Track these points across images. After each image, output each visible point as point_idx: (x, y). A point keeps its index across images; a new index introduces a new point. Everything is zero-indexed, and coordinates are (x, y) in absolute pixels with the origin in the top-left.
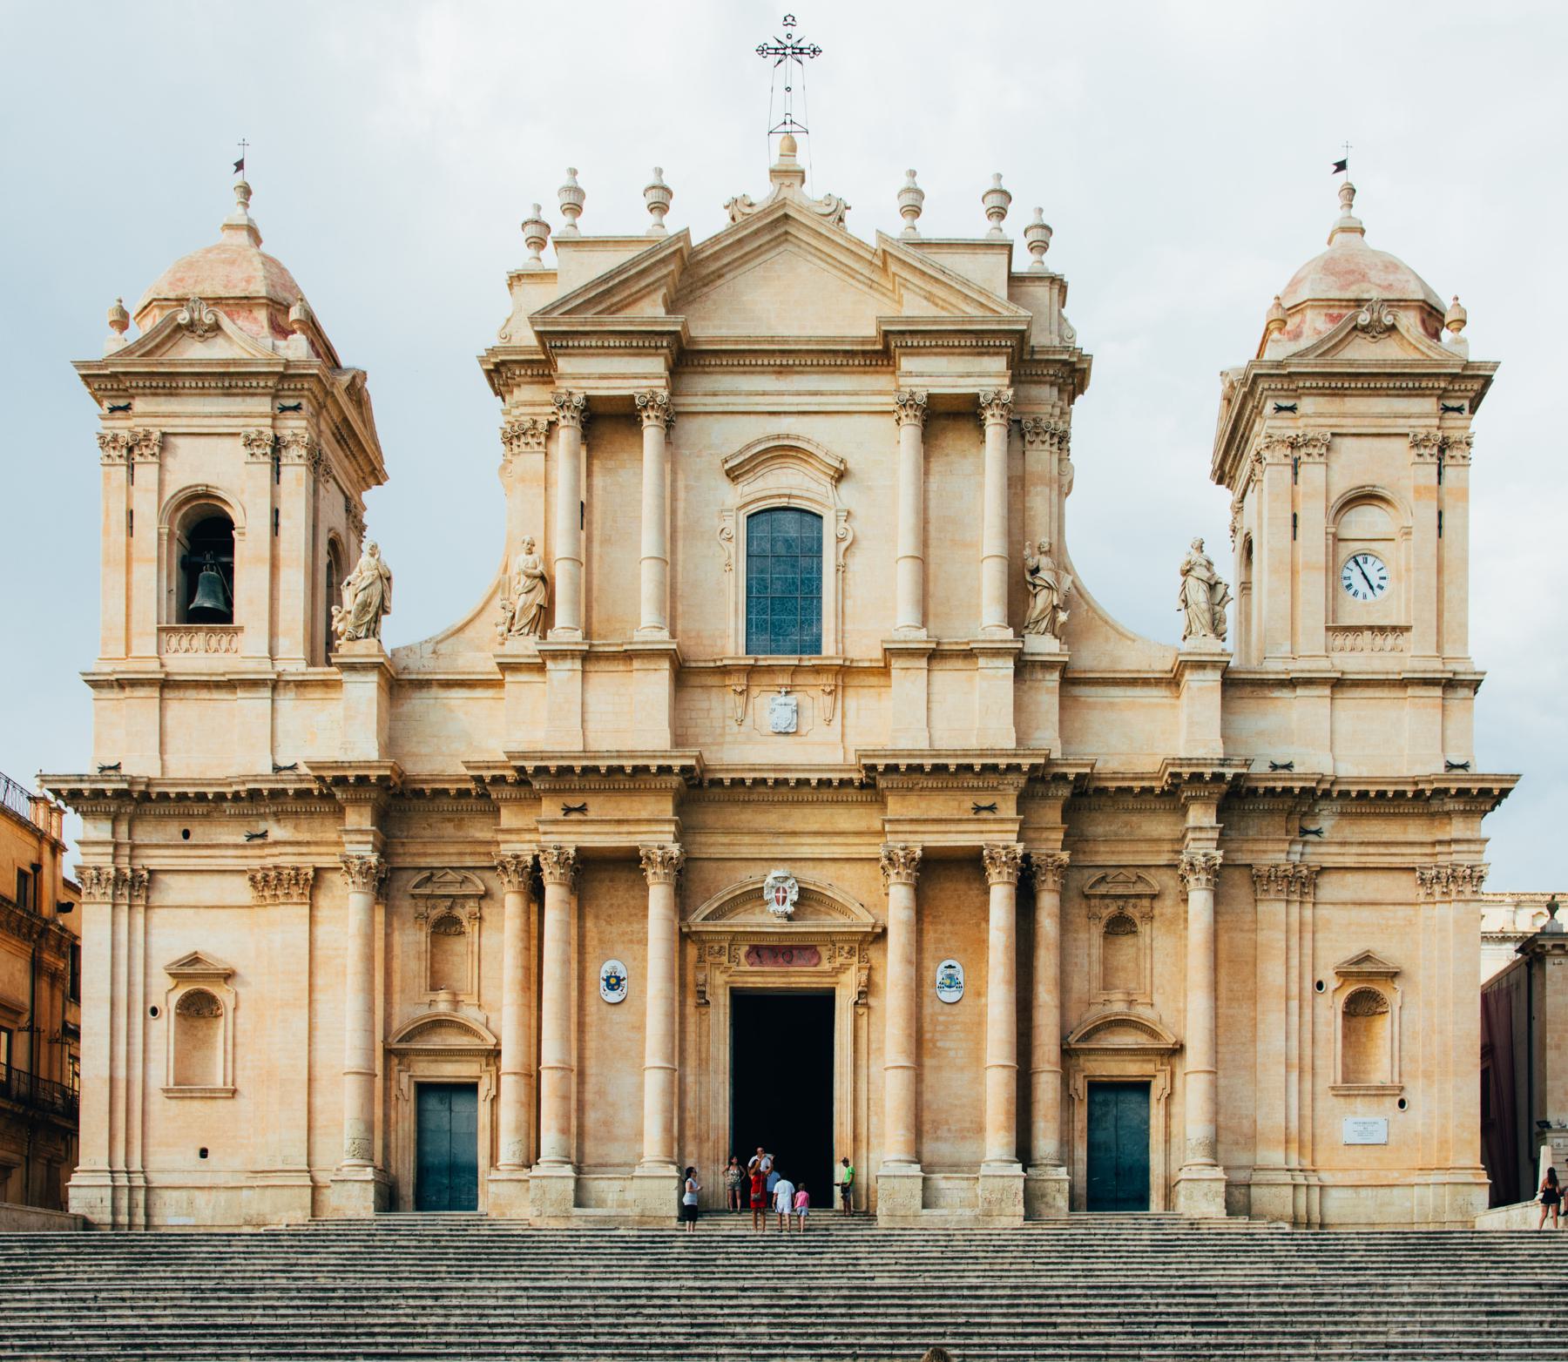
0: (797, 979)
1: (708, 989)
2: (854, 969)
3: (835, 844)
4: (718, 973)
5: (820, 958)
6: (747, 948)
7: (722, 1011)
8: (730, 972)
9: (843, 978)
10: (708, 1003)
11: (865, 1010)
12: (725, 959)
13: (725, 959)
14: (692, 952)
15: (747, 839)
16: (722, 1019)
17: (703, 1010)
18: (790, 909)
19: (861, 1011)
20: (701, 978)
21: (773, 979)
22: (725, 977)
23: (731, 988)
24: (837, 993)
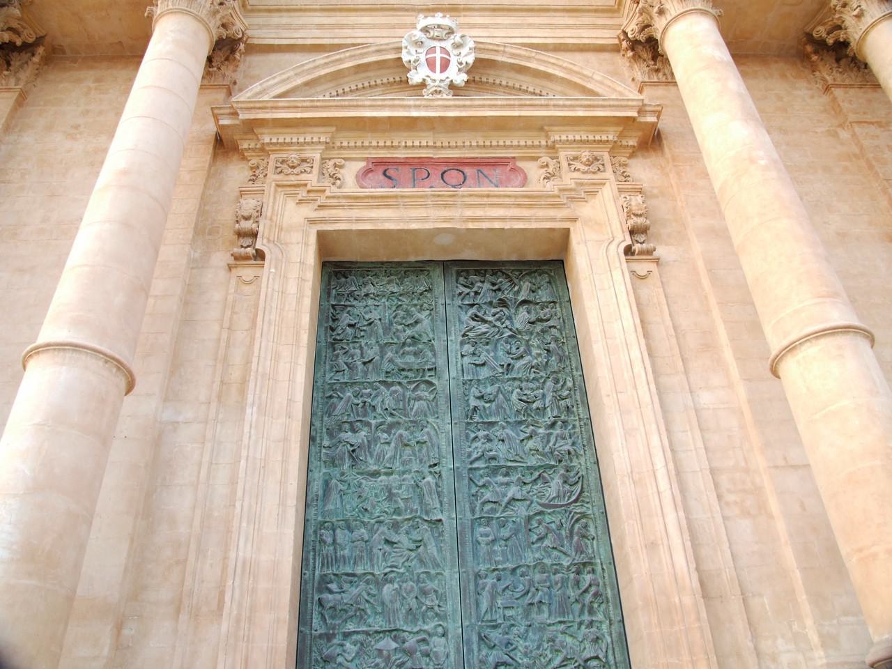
0: (479, 213)
1: (262, 229)
2: (608, 192)
3: (530, 25)
4: (291, 204)
5: (526, 178)
6: (362, 164)
7: (294, 274)
8: (322, 200)
9: (585, 210)
10: (260, 255)
11: (653, 267)
12: (312, 179)
13: (312, 179)
14: (236, 173)
15: (366, 19)
16: (292, 288)
17: (247, 272)
18: (460, 79)
19: (642, 267)
20: (249, 205)
21: (421, 212)
22: (308, 211)
23: (321, 236)
24: (575, 239)
